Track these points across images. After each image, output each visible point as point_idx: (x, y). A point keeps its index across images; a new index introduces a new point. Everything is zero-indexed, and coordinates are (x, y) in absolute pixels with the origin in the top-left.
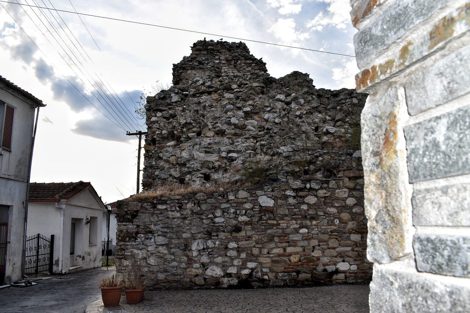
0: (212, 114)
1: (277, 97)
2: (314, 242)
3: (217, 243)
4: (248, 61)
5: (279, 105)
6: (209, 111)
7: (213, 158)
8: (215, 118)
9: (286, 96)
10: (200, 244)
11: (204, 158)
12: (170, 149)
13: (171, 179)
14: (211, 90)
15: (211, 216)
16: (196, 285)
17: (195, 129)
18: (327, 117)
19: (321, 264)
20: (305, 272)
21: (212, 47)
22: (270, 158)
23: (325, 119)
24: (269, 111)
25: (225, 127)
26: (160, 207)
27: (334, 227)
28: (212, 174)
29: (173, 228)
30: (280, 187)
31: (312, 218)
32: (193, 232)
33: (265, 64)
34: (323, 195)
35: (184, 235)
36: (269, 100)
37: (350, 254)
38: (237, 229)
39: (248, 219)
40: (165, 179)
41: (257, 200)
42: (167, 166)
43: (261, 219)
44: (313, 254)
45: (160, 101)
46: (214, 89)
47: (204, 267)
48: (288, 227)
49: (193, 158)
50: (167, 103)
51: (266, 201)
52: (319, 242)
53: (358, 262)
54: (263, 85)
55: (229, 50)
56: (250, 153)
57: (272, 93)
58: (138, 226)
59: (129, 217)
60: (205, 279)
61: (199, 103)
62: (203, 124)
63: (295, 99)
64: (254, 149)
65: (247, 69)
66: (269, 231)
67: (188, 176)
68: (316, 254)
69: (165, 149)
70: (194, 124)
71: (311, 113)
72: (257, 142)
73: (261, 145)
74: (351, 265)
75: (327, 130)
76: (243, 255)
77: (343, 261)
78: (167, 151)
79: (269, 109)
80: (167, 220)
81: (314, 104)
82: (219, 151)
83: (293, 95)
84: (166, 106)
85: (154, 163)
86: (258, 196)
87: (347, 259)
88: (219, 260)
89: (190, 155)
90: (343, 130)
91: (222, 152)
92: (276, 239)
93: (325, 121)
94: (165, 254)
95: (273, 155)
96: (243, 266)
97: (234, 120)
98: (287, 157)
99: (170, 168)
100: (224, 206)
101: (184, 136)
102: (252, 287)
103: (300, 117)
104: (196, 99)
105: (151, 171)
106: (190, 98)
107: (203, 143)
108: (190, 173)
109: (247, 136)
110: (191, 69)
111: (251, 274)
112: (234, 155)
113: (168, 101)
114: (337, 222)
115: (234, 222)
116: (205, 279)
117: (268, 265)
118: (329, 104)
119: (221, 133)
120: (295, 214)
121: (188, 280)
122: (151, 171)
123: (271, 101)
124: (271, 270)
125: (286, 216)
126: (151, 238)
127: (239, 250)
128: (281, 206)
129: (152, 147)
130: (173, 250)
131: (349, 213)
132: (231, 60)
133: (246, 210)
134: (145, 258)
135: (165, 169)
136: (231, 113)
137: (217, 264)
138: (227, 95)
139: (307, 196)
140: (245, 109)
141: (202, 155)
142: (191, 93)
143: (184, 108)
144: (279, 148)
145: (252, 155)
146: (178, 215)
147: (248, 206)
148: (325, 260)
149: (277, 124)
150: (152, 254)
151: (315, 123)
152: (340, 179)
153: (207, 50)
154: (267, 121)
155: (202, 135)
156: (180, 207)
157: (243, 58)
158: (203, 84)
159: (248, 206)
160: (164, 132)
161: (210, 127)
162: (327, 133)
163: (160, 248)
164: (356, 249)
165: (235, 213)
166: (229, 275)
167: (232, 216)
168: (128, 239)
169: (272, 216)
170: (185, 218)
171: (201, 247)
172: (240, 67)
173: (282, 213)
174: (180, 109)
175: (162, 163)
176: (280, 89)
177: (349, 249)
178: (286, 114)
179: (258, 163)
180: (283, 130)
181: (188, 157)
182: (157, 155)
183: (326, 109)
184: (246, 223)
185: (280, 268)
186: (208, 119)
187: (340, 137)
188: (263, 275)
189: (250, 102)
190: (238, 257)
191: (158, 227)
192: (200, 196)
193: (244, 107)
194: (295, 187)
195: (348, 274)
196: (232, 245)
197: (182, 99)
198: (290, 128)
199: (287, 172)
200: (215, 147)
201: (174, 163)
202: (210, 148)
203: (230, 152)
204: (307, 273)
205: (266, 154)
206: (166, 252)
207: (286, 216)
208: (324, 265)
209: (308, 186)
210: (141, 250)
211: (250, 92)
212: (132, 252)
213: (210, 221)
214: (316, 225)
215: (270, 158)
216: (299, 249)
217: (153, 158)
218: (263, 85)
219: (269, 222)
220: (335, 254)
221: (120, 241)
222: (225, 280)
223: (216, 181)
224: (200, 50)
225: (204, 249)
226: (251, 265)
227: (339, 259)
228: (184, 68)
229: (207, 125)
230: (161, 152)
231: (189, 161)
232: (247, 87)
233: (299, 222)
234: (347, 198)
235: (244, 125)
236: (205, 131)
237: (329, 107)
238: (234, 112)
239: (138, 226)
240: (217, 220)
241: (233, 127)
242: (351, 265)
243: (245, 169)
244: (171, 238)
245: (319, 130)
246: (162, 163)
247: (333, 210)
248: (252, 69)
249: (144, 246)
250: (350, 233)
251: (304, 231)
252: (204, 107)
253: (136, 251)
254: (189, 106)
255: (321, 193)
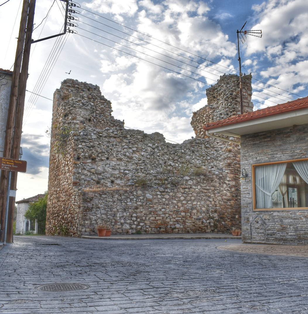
0: (116, 149)
1: (149, 145)
2: (167, 215)
3: (128, 214)
4: (102, 101)
5: (149, 149)
6: (115, 148)
7: (117, 172)
8: (118, 152)
9: (153, 145)
10: (121, 214)
11: (111, 172)
12: (90, 164)
13: (92, 181)
14: (116, 136)
15: (125, 201)
16: (118, 233)
17: (106, 156)
18: (171, 158)
19: (169, 225)
20: (163, 228)
21: (78, 86)
22: (145, 175)
23: (170, 158)
24: (144, 151)
25: (123, 157)
26: (103, 196)
27: (175, 209)
28: (115, 181)
29: (109, 206)
30: (155, 190)
31: (167, 205)
32: (118, 208)
33: (111, 103)
34: (171, 195)
35: (114, 210)
36: (144, 146)
37: (181, 221)
38: (137, 208)
39: (141, 204)
40: (89, 181)
41: (145, 195)
42: (89, 174)
43: (146, 204)
44: (166, 220)
45: (84, 136)
46: (118, 136)
47: (122, 224)
48: (157, 208)
49: (105, 171)
50: (89, 138)
51: (149, 196)
52: (169, 215)
53: (184, 225)
54: (142, 138)
55: (89, 90)
56: (135, 172)
57: (146, 142)
58: (93, 205)
59: (89, 200)
60: (122, 230)
61: (109, 142)
62: (110, 153)
63: (157, 147)
64: (137, 170)
65: (101, 106)
66: (150, 210)
67: (103, 180)
68: (168, 220)
69: (87, 164)
70: (106, 153)
71: (164, 155)
72: (137, 166)
73: (141, 168)
74: (181, 225)
75: (170, 164)
76: (139, 220)
77: (178, 224)
78: (88, 166)
79: (144, 150)
80: (106, 202)
81: (165, 151)
82: (120, 169)
83: (156, 145)
84: (88, 140)
85: (80, 171)
86: (146, 194)
87: (179, 223)
88: (128, 221)
89: (104, 170)
90: (177, 165)
91: (121, 170)
92: (152, 213)
93: (169, 159)
94: (105, 218)
95: (147, 174)
96: (138, 225)
97: (127, 154)
98: (155, 176)
99: (91, 175)
100: (131, 197)
101: (98, 158)
102: (142, 234)
103: (159, 156)
104: (107, 139)
105: (78, 175)
106: (104, 138)
107: (111, 164)
108: (103, 179)
109: (133, 163)
110: (79, 108)
111: (141, 228)
112: (127, 172)
113: (89, 137)
114: (176, 207)
115: (136, 205)
116: (122, 230)
117: (149, 224)
118: (171, 151)
119: (121, 160)
120: (160, 203)
121: (115, 230)
122: (78, 175)
123: (145, 146)
124: (150, 227)
125: (157, 203)
126: (99, 211)
127: (137, 217)
128: (155, 198)
129: (79, 162)
130: (108, 217)
131: (181, 203)
132: (91, 99)
133: (141, 199)
134: (96, 220)
135: (88, 175)
136: (126, 150)
137: (127, 223)
138: (125, 140)
139: (165, 195)
140: (133, 149)
141: (111, 170)
142: (104, 135)
143: (99, 143)
144: (149, 171)
145: (136, 173)
146: (111, 200)
147: (141, 198)
148: (171, 223)
149: (148, 158)
150: (99, 218)
151: (165, 160)
152: (179, 188)
153: (74, 87)
154: (143, 156)
155: (110, 159)
156: (112, 197)
157: (99, 98)
158: (113, 132)
159: (141, 198)
160: (87, 154)
161: (115, 156)
162: (170, 165)
163: (103, 215)
164: (183, 219)
165: (136, 201)
166: (132, 228)
167: (135, 202)
168: (88, 211)
169: (151, 202)
170: (114, 202)
171: (121, 216)
172: (97, 104)
173: (155, 202)
174: (97, 143)
175: (86, 172)
176: (151, 141)
177: (180, 219)
178: (152, 154)
179: (139, 177)
180: (151, 162)
181: (103, 170)
182: (83, 167)
183: (170, 154)
184: (141, 206)
185: (153, 226)
186: (114, 151)
187: (175, 168)
188: (146, 229)
189: (136, 146)
190: (136, 221)
191: (102, 206)
192: (121, 192)
193: (133, 147)
194: (161, 191)
195: (179, 229)
196: (134, 215)
197: (98, 138)
198: (155, 162)
199: (156, 183)
200: (117, 167)
201: (94, 173)
202: (115, 167)
203: (125, 170)
204: (164, 228)
205: (143, 173)
206: (105, 217)
207: (157, 203)
208: (171, 225)
209: (166, 190)
210: (94, 216)
211: (137, 140)
212: (90, 217)
213: (125, 204)
214: (168, 208)
215: (145, 175)
216: (161, 218)
217: (79, 168)
218: (142, 138)
219: (150, 205)
220: (175, 221)
221: (84, 211)
222: (130, 231)
223: (118, 185)
224: (69, 86)
225: (122, 216)
226: (141, 224)
227: (176, 223)
228: (75, 107)
229: (112, 154)
230: (85, 166)
231: (104, 173)
232: (134, 138)
233: (162, 206)
234: (181, 197)
235: (132, 157)
236: (111, 157)
237: (172, 153)
238: (127, 150)
239: (93, 205)
240: (128, 203)
241: (127, 157)
242: (181, 225)
243: (133, 179)
244: (108, 211)
245: (166, 163)
246: (86, 172)
247: (175, 202)
248: (105, 107)
249: (95, 214)
250: (181, 212)
251: (163, 210)
252: (113, 145)
253: (91, 216)
254: (103, 143)
255: (171, 194)
